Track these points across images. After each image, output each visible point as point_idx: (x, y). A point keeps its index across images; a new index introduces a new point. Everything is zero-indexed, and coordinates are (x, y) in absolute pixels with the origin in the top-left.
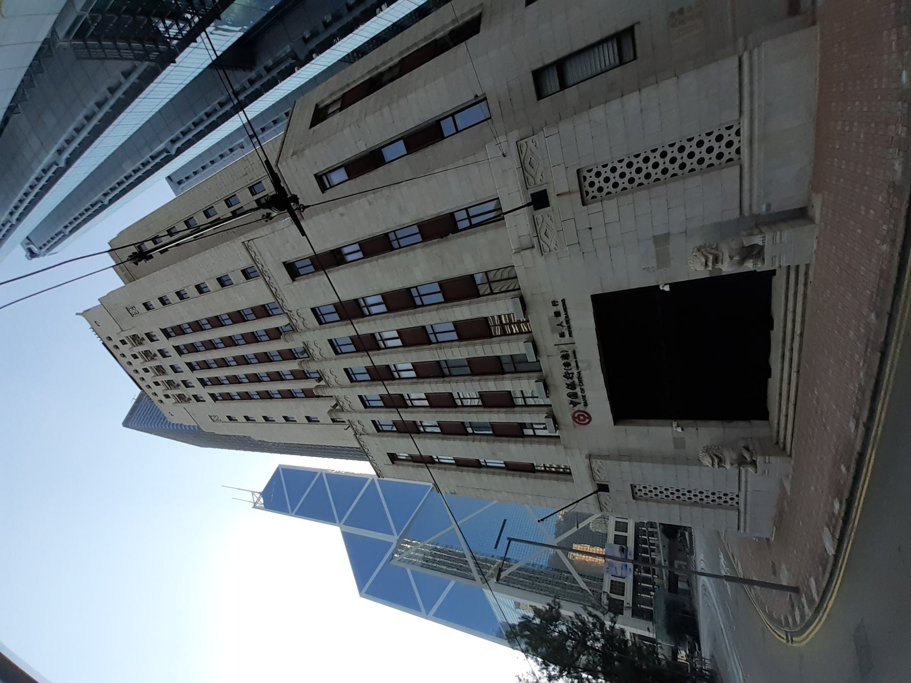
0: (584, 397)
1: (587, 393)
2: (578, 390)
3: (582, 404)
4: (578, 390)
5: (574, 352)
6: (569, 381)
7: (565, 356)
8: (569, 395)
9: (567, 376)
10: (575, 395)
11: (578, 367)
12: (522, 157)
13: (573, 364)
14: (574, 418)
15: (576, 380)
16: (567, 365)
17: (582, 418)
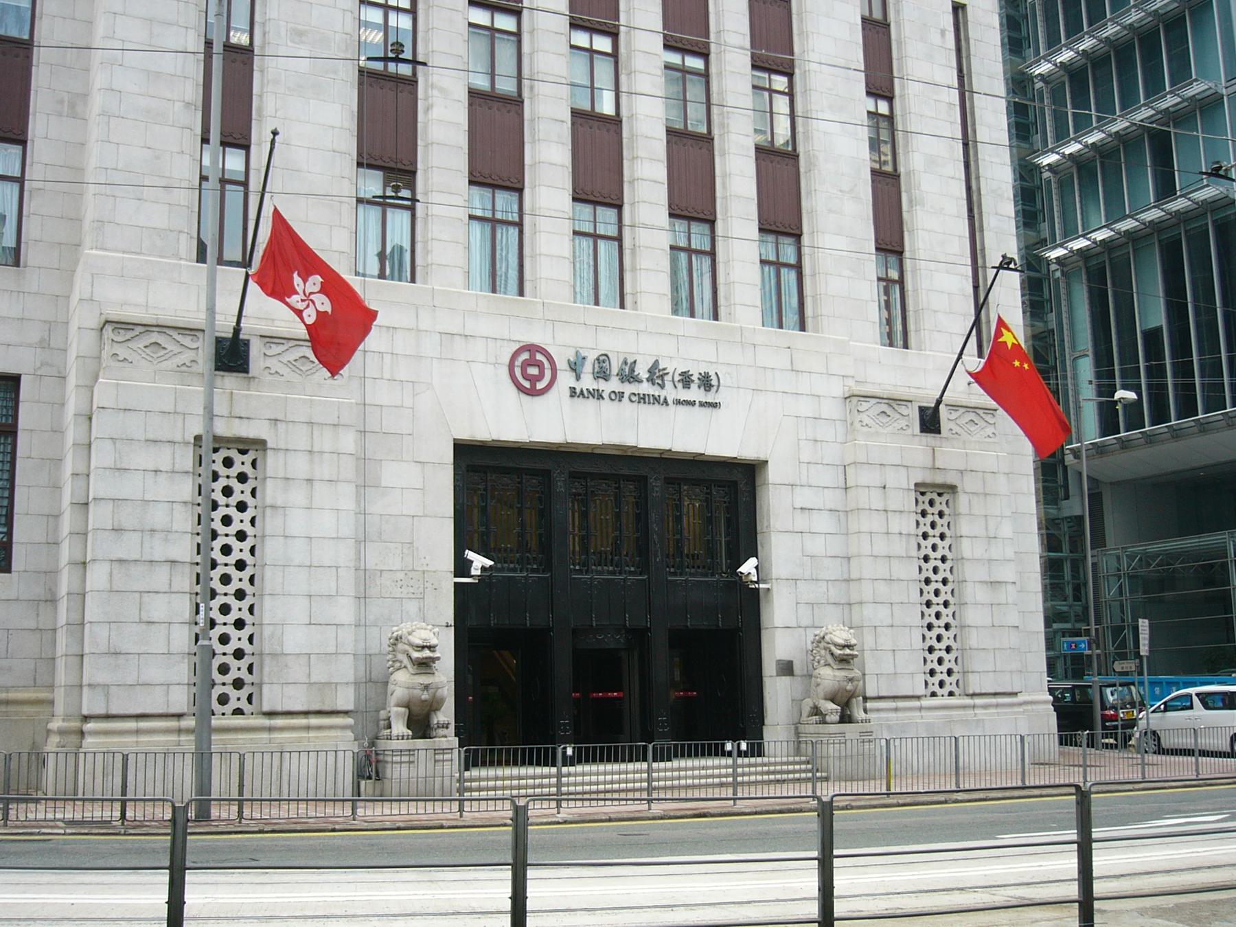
0: (600, 397)
1: (606, 403)
2: (614, 385)
3: (573, 383)
4: (614, 385)
5: (714, 405)
6: (642, 371)
7: (706, 382)
8: (603, 360)
9: (656, 375)
10: (602, 374)
11: (678, 402)
12: (981, 412)
13: (684, 395)
14: (532, 348)
15: (646, 388)
16: (686, 380)
17: (533, 371)
